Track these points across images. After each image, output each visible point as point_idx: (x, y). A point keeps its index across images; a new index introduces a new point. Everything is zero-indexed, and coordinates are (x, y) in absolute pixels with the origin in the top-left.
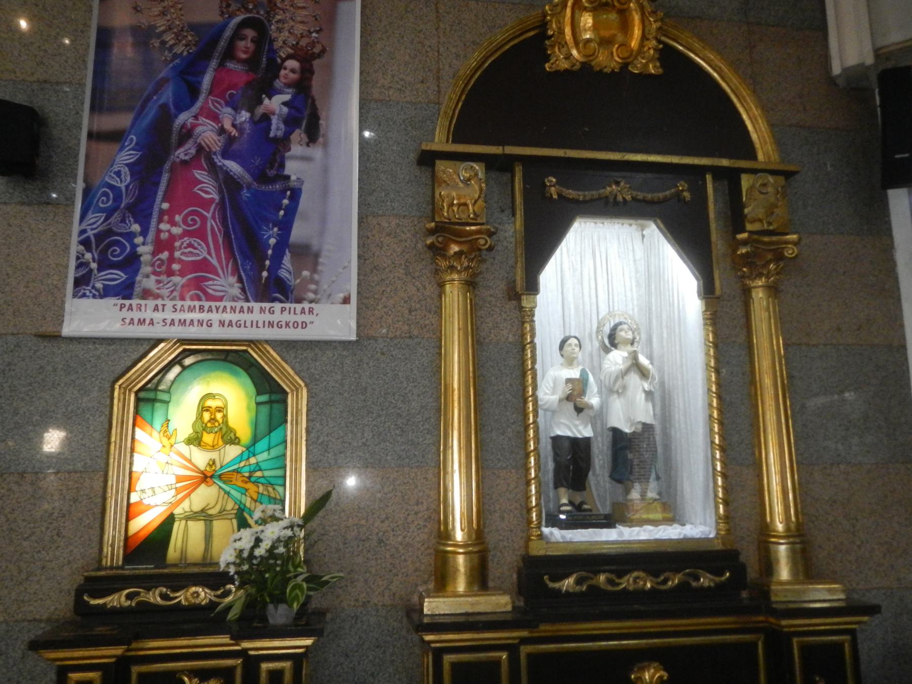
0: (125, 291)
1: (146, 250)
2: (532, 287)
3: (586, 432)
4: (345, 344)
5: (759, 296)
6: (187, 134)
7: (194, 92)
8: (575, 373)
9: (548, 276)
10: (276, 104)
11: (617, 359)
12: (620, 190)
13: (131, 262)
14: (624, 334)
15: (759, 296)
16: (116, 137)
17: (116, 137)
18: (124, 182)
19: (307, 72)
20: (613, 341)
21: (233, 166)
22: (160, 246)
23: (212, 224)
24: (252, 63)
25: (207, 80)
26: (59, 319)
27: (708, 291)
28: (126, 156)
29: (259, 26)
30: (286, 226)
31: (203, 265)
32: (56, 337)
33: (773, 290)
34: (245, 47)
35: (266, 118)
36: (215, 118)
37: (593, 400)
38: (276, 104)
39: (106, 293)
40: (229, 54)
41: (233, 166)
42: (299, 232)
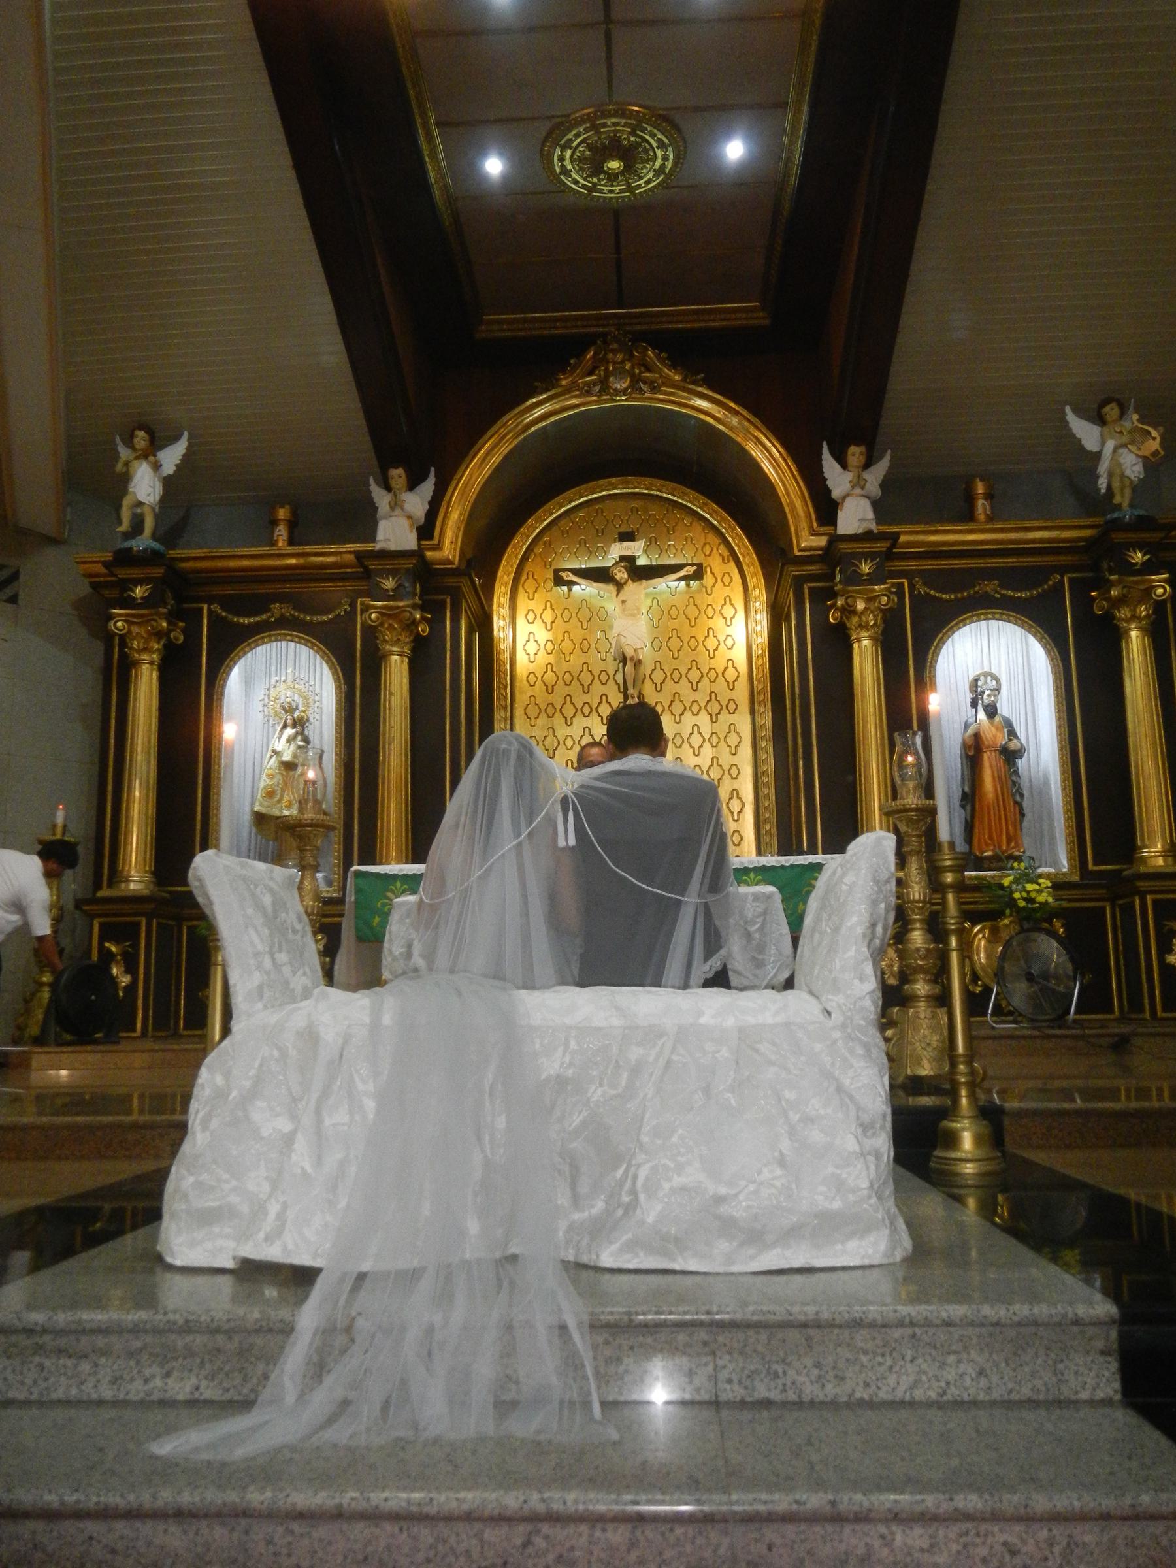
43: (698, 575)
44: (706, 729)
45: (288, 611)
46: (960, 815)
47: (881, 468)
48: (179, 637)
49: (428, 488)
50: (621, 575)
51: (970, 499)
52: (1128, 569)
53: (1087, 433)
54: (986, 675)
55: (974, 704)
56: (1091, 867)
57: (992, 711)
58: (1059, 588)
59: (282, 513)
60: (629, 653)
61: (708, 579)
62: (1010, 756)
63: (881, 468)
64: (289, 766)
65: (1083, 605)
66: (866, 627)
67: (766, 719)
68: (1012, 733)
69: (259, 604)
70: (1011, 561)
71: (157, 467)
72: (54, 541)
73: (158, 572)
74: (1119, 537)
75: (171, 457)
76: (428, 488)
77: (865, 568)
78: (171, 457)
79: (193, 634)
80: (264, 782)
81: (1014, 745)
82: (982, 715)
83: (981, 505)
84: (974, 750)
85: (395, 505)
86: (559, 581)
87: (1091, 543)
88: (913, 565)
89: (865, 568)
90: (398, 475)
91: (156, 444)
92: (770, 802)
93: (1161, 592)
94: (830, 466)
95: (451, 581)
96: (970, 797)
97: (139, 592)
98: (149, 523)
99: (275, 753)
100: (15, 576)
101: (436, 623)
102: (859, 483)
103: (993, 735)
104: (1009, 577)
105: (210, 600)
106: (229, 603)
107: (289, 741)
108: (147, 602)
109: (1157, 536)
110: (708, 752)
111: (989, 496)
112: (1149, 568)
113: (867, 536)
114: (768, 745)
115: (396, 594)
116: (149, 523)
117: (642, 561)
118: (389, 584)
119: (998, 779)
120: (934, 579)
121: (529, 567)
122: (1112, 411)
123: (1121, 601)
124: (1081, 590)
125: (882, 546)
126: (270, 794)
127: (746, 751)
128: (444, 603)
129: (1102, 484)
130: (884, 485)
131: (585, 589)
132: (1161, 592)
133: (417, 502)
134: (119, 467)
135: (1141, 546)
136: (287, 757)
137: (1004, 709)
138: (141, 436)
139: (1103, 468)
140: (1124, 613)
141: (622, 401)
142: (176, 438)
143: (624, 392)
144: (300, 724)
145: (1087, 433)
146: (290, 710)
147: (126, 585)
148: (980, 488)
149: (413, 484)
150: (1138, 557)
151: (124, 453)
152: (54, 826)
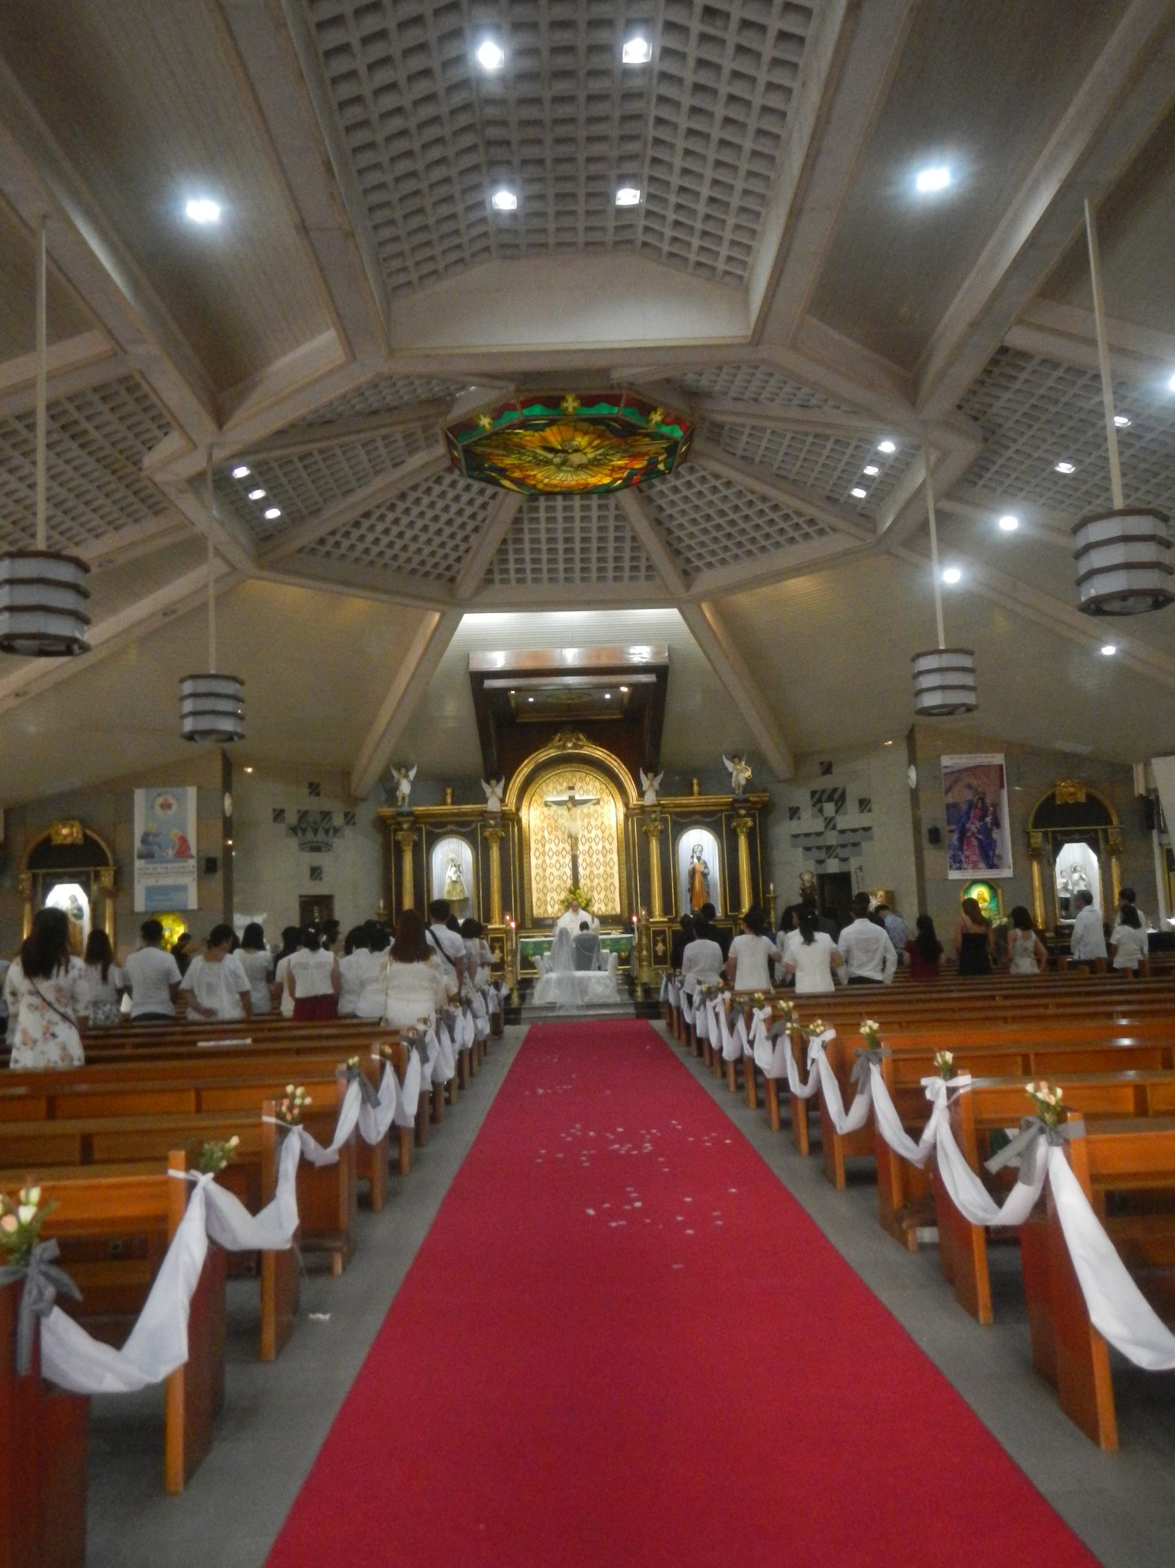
0: (960, 868)
1: (963, 859)
2: (1055, 861)
3: (1068, 896)
4: (1010, 878)
5: (1114, 860)
6: (969, 829)
7: (969, 818)
8: (1065, 881)
9: (1058, 860)
10: (988, 819)
11: (1076, 876)
12: (1076, 836)
13: (960, 862)
14: (1078, 869)
15: (1114, 860)
16: (952, 831)
17: (952, 831)
18: (956, 842)
19: (995, 810)
20: (1075, 870)
21: (980, 836)
22: (967, 857)
23: (977, 852)
24: (982, 810)
25: (972, 815)
26: (947, 875)
27: (1099, 860)
28: (955, 837)
29: (982, 799)
30: (994, 851)
31: (977, 861)
32: (947, 880)
33: (1118, 859)
34: (980, 805)
35: (986, 824)
36: (973, 823)
37: (1070, 887)
38: (988, 819)
39: (957, 869)
40: (976, 807)
41: (980, 836)
42: (997, 852)
43: (598, 802)
44: (602, 860)
45: (453, 827)
46: (688, 896)
47: (660, 777)
48: (415, 837)
49: (502, 783)
50: (570, 805)
51: (692, 786)
52: (740, 816)
53: (729, 765)
54: (698, 845)
55: (692, 857)
56: (729, 913)
57: (699, 859)
58: (721, 817)
59: (449, 791)
60: (573, 835)
61: (601, 803)
62: (705, 875)
63: (660, 777)
64: (455, 882)
65: (728, 825)
66: (654, 836)
67: (624, 857)
68: (706, 867)
69: (443, 825)
70: (706, 808)
71: (409, 781)
72: (363, 800)
73: (412, 818)
74: (737, 805)
75: (412, 773)
76: (502, 783)
77: (653, 816)
78: (412, 773)
79: (420, 836)
80: (447, 888)
81: (706, 871)
82: (695, 860)
83: (696, 788)
84: (693, 873)
85: (493, 792)
86: (546, 804)
87: (731, 804)
88: (671, 810)
89: (653, 816)
90: (493, 782)
91: (408, 770)
92: (624, 888)
93: (750, 824)
94: (643, 776)
95: (511, 816)
96: (691, 890)
97: (405, 826)
98: (407, 800)
99: (451, 878)
100: (353, 816)
101: (507, 832)
102: (651, 785)
103: (700, 868)
104: (704, 814)
105: (425, 823)
106: (431, 824)
107: (455, 872)
108: (409, 829)
109: (749, 805)
110: (602, 869)
111: (699, 785)
112: (745, 816)
113: (654, 806)
114: (624, 867)
115: (496, 826)
116: (407, 800)
117: (578, 797)
118: (492, 822)
119: (701, 883)
120: (678, 814)
121: (534, 798)
122: (736, 760)
123: (738, 826)
124: (729, 818)
125: (658, 809)
126: (449, 892)
127: (616, 868)
128: (508, 825)
129: (733, 785)
130: (660, 785)
131: (554, 807)
132: (750, 824)
133: (499, 790)
134: (396, 781)
135: (742, 808)
136: (454, 878)
137: (703, 857)
138: (403, 770)
139: (733, 780)
140: (738, 830)
141: (570, 751)
142: (412, 767)
143: (570, 748)
144: (458, 867)
145: (729, 765)
146: (453, 860)
147: (399, 824)
148: (695, 781)
149: (498, 781)
150: (743, 812)
151: (395, 774)
152: (379, 908)
